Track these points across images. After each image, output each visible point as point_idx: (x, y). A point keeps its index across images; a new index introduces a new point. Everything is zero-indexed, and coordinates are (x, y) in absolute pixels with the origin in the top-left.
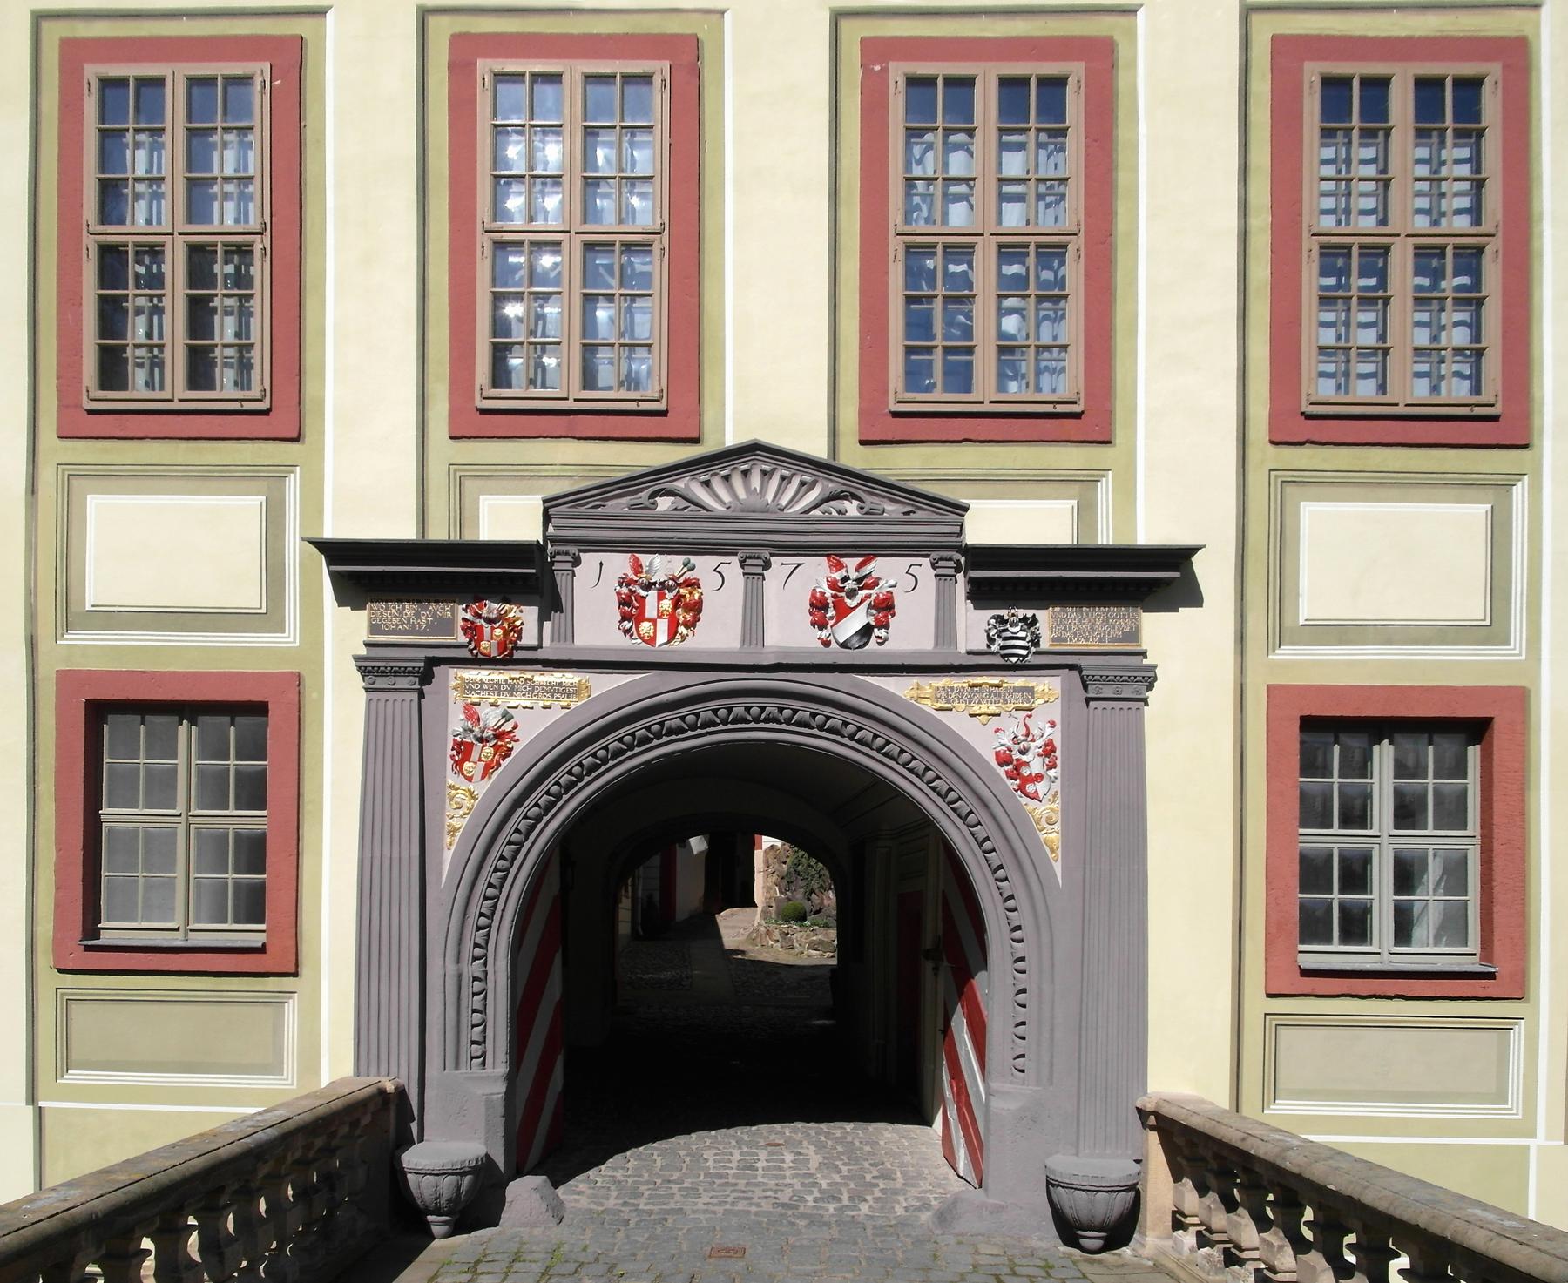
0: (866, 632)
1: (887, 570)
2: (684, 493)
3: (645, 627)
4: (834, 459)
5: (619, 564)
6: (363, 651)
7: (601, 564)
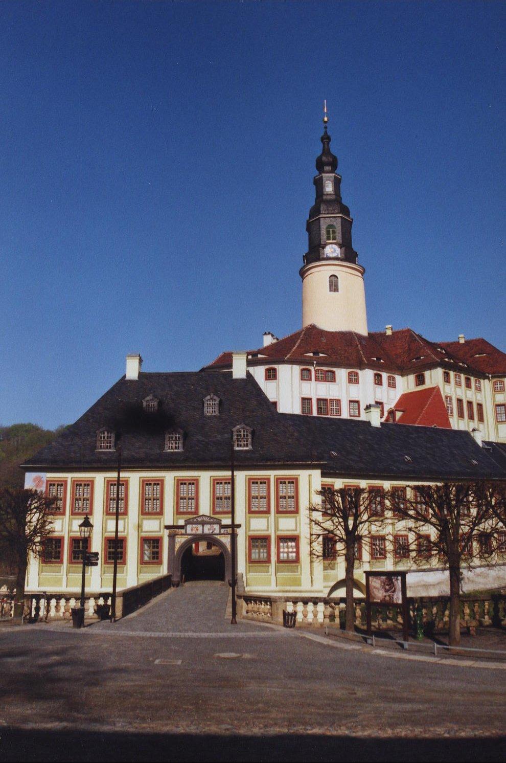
0: (213, 532)
5: (191, 526)
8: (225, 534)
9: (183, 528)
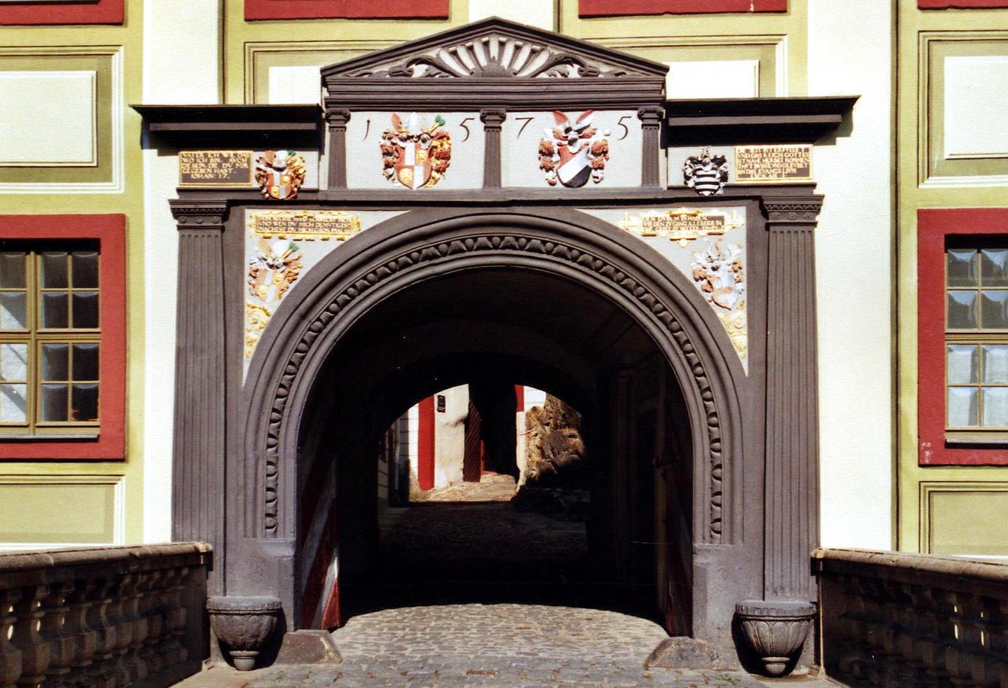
0: (585, 174)
1: (604, 124)
2: (437, 62)
3: (405, 173)
4: (559, 31)
5: (383, 121)
6: (176, 196)
7: (368, 121)
8: (698, 199)
9: (312, 142)
